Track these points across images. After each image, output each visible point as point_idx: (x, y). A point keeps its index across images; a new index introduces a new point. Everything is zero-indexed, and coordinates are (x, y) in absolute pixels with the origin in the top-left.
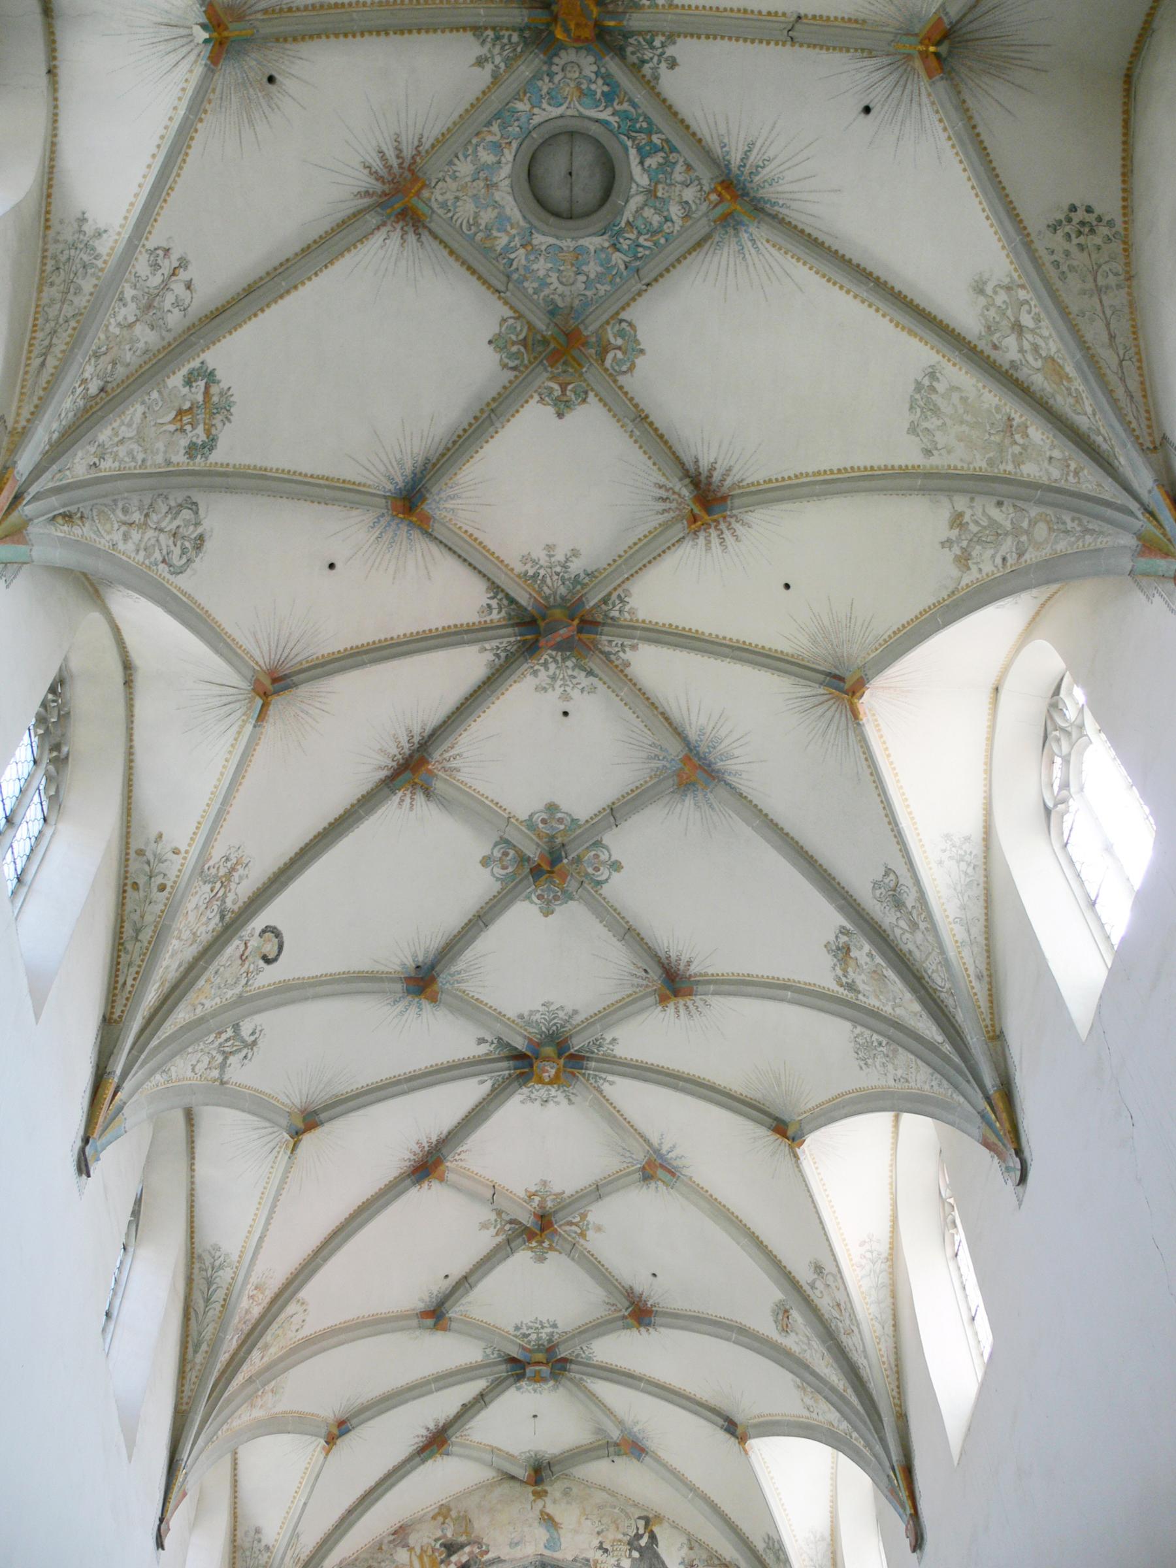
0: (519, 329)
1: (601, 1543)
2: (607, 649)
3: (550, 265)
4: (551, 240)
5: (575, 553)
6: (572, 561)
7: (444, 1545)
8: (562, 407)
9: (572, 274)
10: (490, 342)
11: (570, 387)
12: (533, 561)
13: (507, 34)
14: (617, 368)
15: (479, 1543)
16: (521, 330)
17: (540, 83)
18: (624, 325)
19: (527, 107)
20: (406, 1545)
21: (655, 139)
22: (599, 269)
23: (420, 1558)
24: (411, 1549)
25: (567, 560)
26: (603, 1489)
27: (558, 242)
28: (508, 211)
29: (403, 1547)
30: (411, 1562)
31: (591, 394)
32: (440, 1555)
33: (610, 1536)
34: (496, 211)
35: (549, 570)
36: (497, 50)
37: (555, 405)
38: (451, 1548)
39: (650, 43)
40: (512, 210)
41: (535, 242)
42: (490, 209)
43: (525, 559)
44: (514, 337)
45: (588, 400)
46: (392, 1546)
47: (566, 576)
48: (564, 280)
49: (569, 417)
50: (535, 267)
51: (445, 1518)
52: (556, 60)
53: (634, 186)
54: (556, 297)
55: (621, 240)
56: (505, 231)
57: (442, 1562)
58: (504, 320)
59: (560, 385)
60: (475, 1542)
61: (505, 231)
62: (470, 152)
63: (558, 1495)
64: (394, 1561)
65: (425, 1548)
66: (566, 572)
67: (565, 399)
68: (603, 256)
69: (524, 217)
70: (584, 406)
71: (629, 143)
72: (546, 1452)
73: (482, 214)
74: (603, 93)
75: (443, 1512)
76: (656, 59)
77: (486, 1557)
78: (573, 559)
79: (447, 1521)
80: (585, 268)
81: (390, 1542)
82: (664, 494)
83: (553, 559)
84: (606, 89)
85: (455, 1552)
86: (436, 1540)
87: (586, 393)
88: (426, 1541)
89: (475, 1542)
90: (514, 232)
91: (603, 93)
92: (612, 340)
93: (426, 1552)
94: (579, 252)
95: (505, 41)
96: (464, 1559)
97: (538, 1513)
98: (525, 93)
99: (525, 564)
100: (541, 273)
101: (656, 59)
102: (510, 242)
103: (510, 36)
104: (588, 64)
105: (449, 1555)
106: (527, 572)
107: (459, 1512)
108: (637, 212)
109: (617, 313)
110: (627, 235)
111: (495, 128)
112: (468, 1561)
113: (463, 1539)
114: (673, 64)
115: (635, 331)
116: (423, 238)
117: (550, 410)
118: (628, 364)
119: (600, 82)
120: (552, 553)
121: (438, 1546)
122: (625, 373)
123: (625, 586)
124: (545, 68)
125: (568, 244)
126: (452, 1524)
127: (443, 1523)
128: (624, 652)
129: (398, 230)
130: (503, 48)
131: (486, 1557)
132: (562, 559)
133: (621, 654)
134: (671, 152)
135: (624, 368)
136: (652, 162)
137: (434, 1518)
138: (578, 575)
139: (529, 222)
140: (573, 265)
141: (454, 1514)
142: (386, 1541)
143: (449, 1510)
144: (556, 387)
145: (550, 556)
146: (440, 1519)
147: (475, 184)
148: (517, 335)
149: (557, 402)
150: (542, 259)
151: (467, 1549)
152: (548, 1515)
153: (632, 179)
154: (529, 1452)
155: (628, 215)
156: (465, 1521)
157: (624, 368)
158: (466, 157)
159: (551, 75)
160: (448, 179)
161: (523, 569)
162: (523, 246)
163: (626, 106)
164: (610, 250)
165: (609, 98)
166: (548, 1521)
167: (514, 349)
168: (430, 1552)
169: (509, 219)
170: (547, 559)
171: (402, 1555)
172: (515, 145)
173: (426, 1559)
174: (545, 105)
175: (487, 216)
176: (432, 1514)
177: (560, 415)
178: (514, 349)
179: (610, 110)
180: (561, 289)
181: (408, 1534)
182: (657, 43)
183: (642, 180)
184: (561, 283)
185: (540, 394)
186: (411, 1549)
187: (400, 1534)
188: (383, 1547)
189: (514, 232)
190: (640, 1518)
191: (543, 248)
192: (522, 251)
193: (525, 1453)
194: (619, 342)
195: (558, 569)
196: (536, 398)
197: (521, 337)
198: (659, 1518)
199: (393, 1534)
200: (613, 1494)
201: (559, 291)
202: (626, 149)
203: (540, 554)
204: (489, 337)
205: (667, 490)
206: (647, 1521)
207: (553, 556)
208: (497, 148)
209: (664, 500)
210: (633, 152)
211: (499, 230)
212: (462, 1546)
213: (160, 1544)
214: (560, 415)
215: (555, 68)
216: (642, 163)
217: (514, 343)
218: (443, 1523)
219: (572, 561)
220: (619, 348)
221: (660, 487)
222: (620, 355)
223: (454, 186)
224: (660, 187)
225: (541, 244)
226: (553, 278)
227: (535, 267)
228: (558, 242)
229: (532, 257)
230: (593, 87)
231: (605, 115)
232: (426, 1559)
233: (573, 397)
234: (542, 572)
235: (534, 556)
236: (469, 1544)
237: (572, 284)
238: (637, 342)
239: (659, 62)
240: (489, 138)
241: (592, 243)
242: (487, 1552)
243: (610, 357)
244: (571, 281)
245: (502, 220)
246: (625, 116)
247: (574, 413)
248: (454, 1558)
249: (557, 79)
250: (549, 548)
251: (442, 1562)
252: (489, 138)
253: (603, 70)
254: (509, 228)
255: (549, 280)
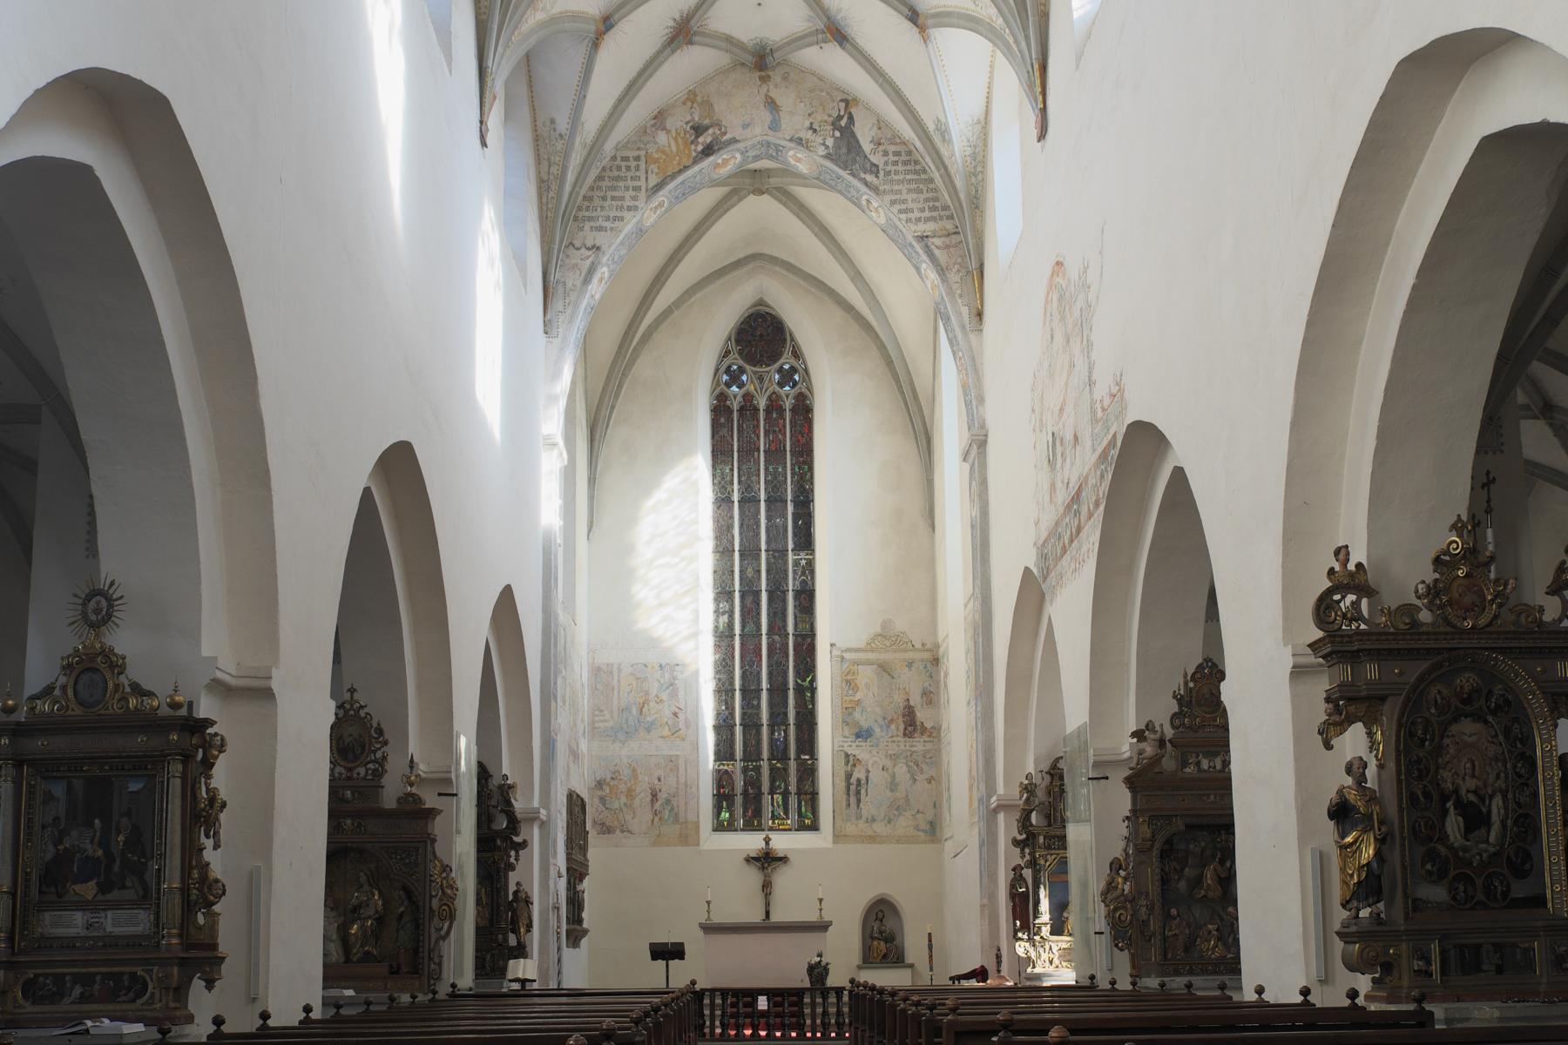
1: (811, 124)
7: (692, 128)
15: (719, 126)
20: (664, 129)
23: (676, 139)
24: (668, 132)
26: (813, 74)
29: (663, 130)
30: (669, 144)
32: (691, 136)
33: (819, 117)
38: (698, 130)
46: (653, 129)
51: (693, 103)
57: (692, 142)
60: (716, 125)
63: (778, 79)
64: (656, 143)
65: (679, 131)
72: (768, 39)
75: (691, 97)
77: (725, 138)
79: (695, 105)
81: (652, 126)
85: (701, 134)
86: (687, 123)
88: (679, 123)
89: (716, 125)
93: (680, 134)
96: (709, 140)
97: (764, 97)
105: (697, 137)
107: (703, 97)
112: (712, 141)
113: (707, 122)
121: (688, 128)
126: (698, 109)
127: (691, 108)
131: (725, 138)
137: (684, 103)
141: (699, 99)
142: (649, 125)
143: (695, 95)
146: (689, 104)
151: (710, 131)
152: (771, 98)
154: (756, 38)
156: (708, 105)
166: (771, 104)
168: (682, 135)
171: (662, 138)
173: (680, 141)
176: (682, 99)
181: (666, 119)
186: (668, 132)
187: (659, 118)
188: (648, 131)
190: (842, 100)
193: (752, 40)
198: (856, 101)
199: (654, 119)
200: (821, 79)
206: (847, 102)
212: (707, 128)
213: (484, 144)
218: (691, 108)
232: (680, 141)
236: (712, 126)
242: (725, 133)
248: (701, 140)
251: (692, 142)
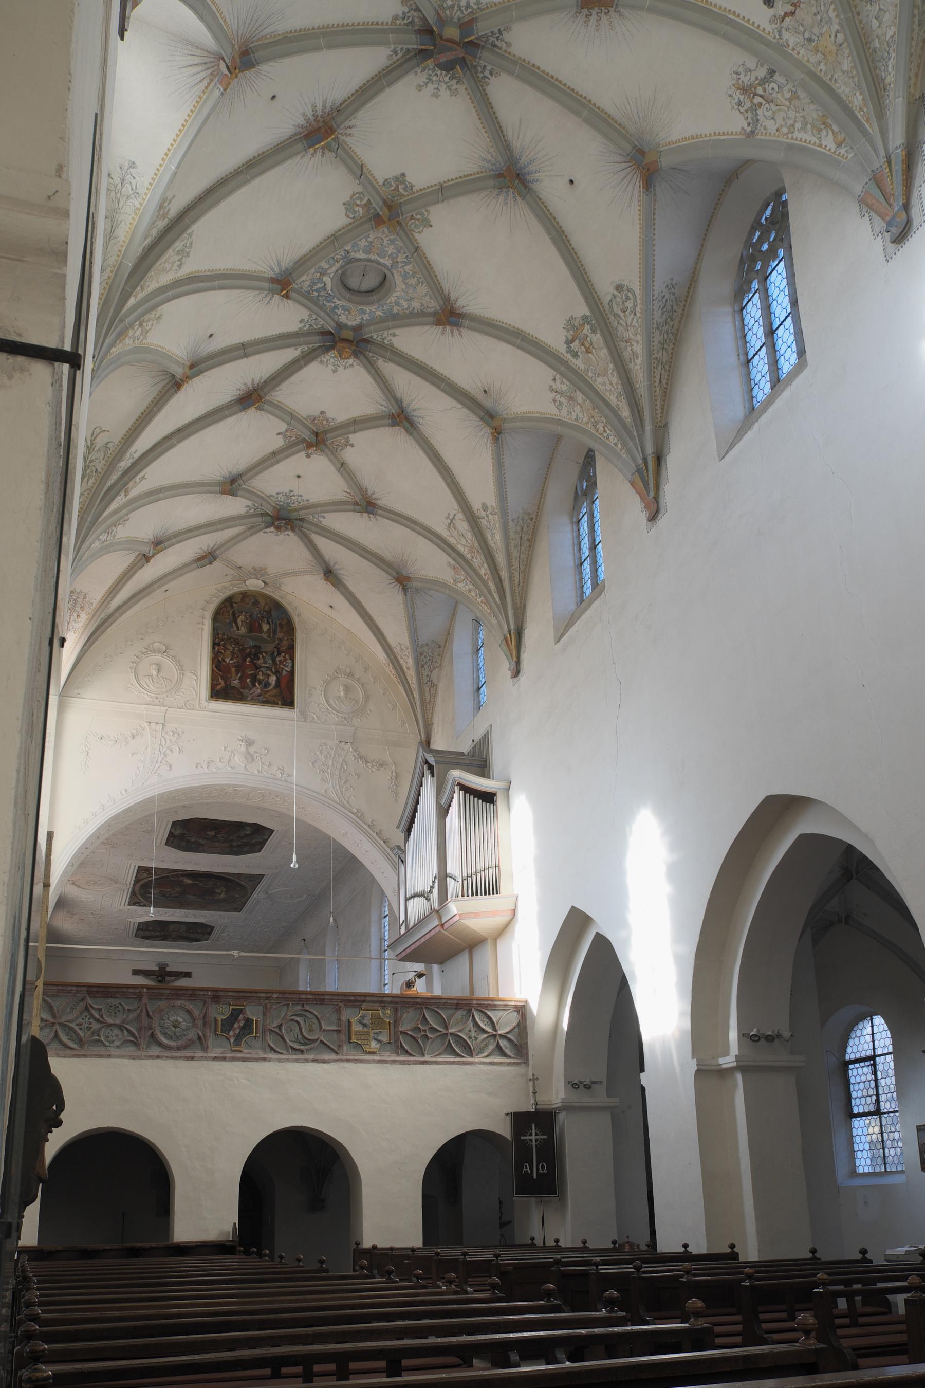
0: (413, 225)
2: (416, 14)
3: (387, 249)
4: (382, 260)
5: (419, 88)
6: (423, 82)
8: (401, 179)
9: (375, 242)
10: (431, 226)
11: (393, 188)
12: (450, 89)
13: (378, 339)
14: (362, 196)
16: (412, 224)
17: (368, 318)
18: (352, 216)
19: (377, 313)
21: (316, 294)
22: (359, 243)
25: (426, 84)
27: (378, 258)
28: (401, 279)
31: (381, 183)
34: (407, 281)
35: (441, 79)
36: (384, 336)
37: (404, 181)
39: (311, 325)
40: (398, 279)
41: (391, 262)
42: (410, 283)
43: (454, 93)
44: (417, 222)
45: (383, 180)
47: (430, 72)
48: (380, 240)
49: (397, 173)
50: (394, 251)
52: (357, 323)
53: (331, 276)
54: (387, 233)
55: (344, 255)
56: (405, 271)
58: (420, 232)
59: (398, 190)
61: (405, 271)
62: (410, 310)
66: (430, 75)
67: (397, 183)
68: (355, 248)
69: (393, 274)
70: (386, 178)
71: (330, 292)
73: (414, 284)
74: (338, 309)
76: (310, 320)
78: (421, 84)
80: (367, 244)
82: (349, 131)
83: (436, 86)
84: (336, 311)
87: (384, 184)
90: (400, 270)
91: (338, 309)
92: (361, 209)
94: (367, 252)
95: (380, 337)
98: (377, 317)
99: (456, 89)
100: (392, 246)
101: (310, 320)
102: (404, 266)
103: (377, 337)
104: (343, 319)
106: (457, 83)
108: (332, 266)
109: (354, 222)
110: (340, 257)
111: (395, 311)
114: (301, 321)
115: (346, 213)
116: (447, 292)
117: (408, 179)
118: (354, 197)
119: (339, 313)
120: (435, 91)
122: (357, 193)
123: (391, 62)
124: (364, 322)
125: (373, 257)
128: (404, 13)
129: (457, 305)
130: (382, 335)
132: (430, 85)
133: (406, 10)
134: (309, 291)
135: (357, 195)
136: (319, 285)
138: (421, 72)
139: (391, 272)
140: (374, 246)
144: (401, 190)
145: (437, 89)
147: (413, 297)
148: (415, 222)
149: (404, 182)
150: (390, 252)
153: (332, 279)
155: (338, 265)
157: (357, 195)
158: (414, 308)
159: (362, 318)
160: (426, 306)
161: (458, 86)
162: (398, 262)
163: (328, 304)
164: (351, 251)
165: (336, 307)
167: (419, 217)
169: (402, 275)
170: (439, 88)
172: (388, 302)
174: (368, 311)
175: (413, 281)
177: (403, 175)
178: (419, 217)
179: (336, 304)
180: (383, 237)
182: (307, 327)
183: (326, 279)
184: (382, 239)
185: (412, 189)
189: (400, 270)
191: (387, 258)
192: (398, 260)
194: (356, 209)
195: (435, 78)
196: (415, 189)
197: (413, 221)
201: (385, 235)
202: (332, 290)
203: (444, 92)
204: (430, 228)
205: (346, 134)
207: (435, 89)
208: (397, 303)
209: (350, 127)
210: (329, 287)
211: (408, 273)
214: (403, 175)
215: (360, 321)
216: (325, 285)
217: (418, 220)
219: (423, 82)
220: (358, 205)
221: (350, 134)
222: (358, 202)
223: (424, 302)
224: (318, 277)
225: (388, 260)
226: (386, 242)
227: (394, 251)
228: (378, 258)
229: (394, 255)
230: (343, 312)
231: (339, 302)
233: (392, 183)
234: (447, 79)
235: (448, 92)
237: (376, 238)
238: (346, 209)
239: (308, 321)
240: (400, 309)
241: (361, 255)
243: (365, 201)
244: (377, 239)
245: (405, 276)
246: (328, 302)
247: (395, 174)
249: (360, 317)
250: (436, 96)
252: (400, 309)
253: (336, 316)
254: (403, 272)
255: (389, 242)
